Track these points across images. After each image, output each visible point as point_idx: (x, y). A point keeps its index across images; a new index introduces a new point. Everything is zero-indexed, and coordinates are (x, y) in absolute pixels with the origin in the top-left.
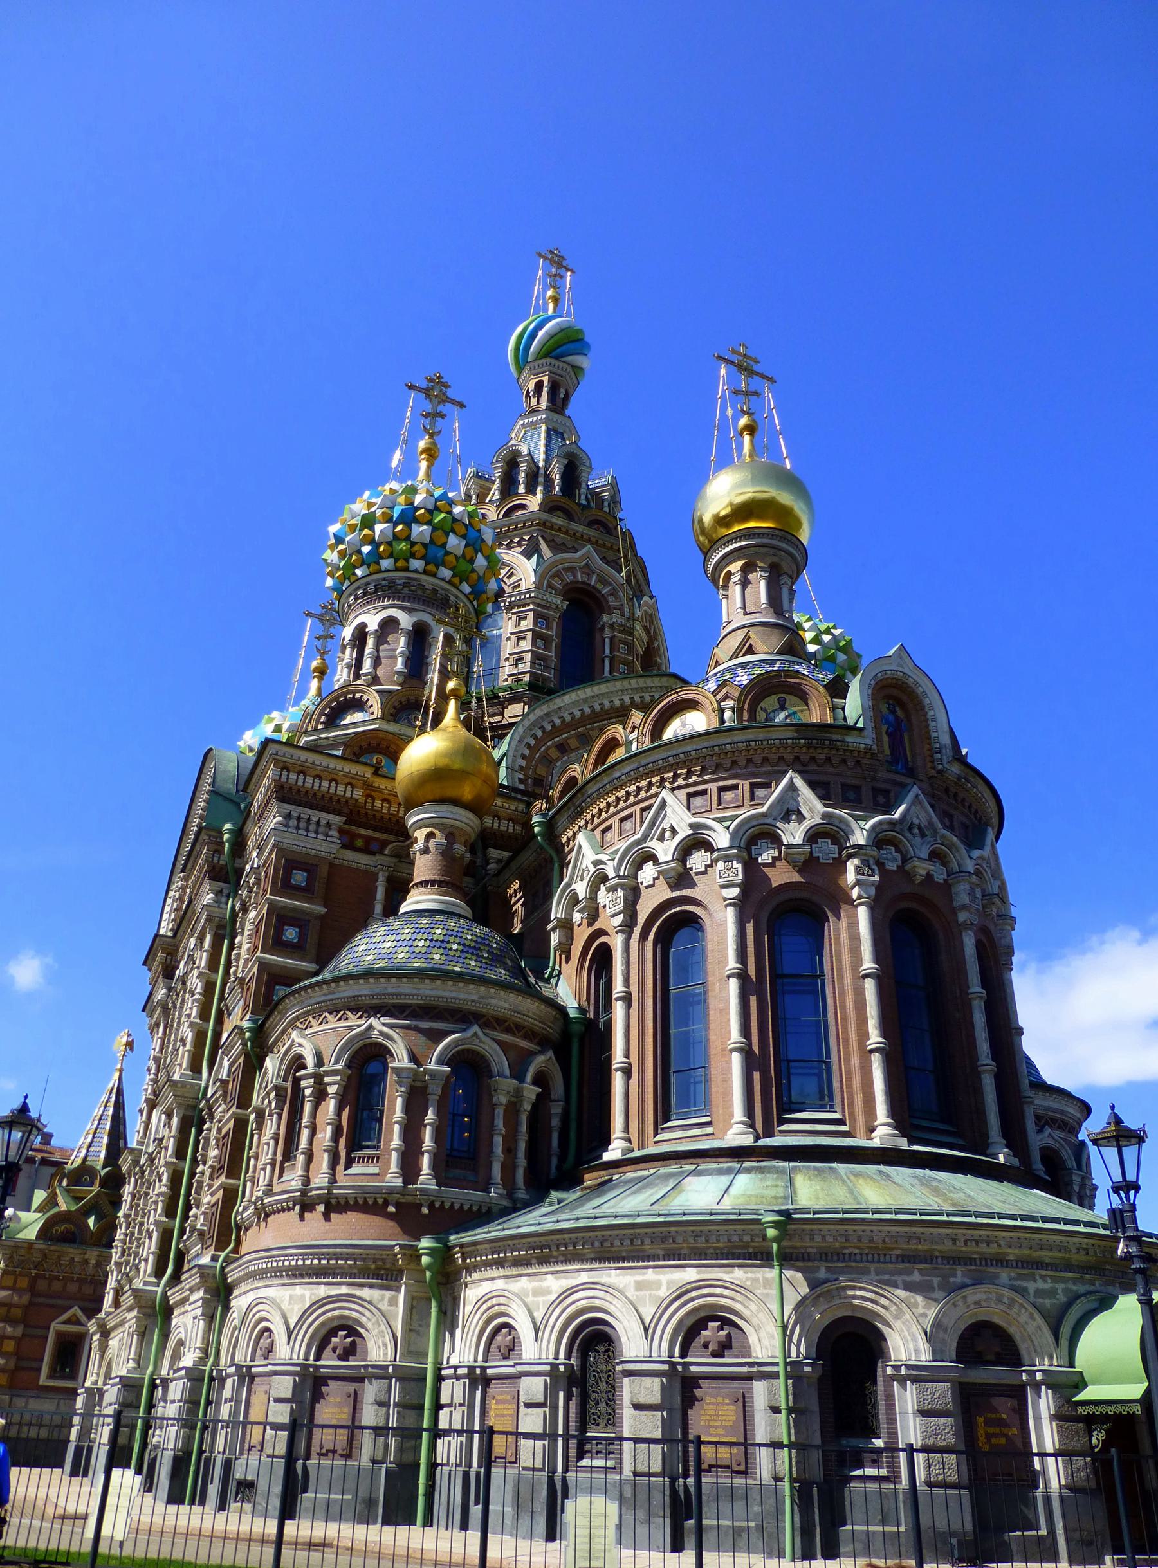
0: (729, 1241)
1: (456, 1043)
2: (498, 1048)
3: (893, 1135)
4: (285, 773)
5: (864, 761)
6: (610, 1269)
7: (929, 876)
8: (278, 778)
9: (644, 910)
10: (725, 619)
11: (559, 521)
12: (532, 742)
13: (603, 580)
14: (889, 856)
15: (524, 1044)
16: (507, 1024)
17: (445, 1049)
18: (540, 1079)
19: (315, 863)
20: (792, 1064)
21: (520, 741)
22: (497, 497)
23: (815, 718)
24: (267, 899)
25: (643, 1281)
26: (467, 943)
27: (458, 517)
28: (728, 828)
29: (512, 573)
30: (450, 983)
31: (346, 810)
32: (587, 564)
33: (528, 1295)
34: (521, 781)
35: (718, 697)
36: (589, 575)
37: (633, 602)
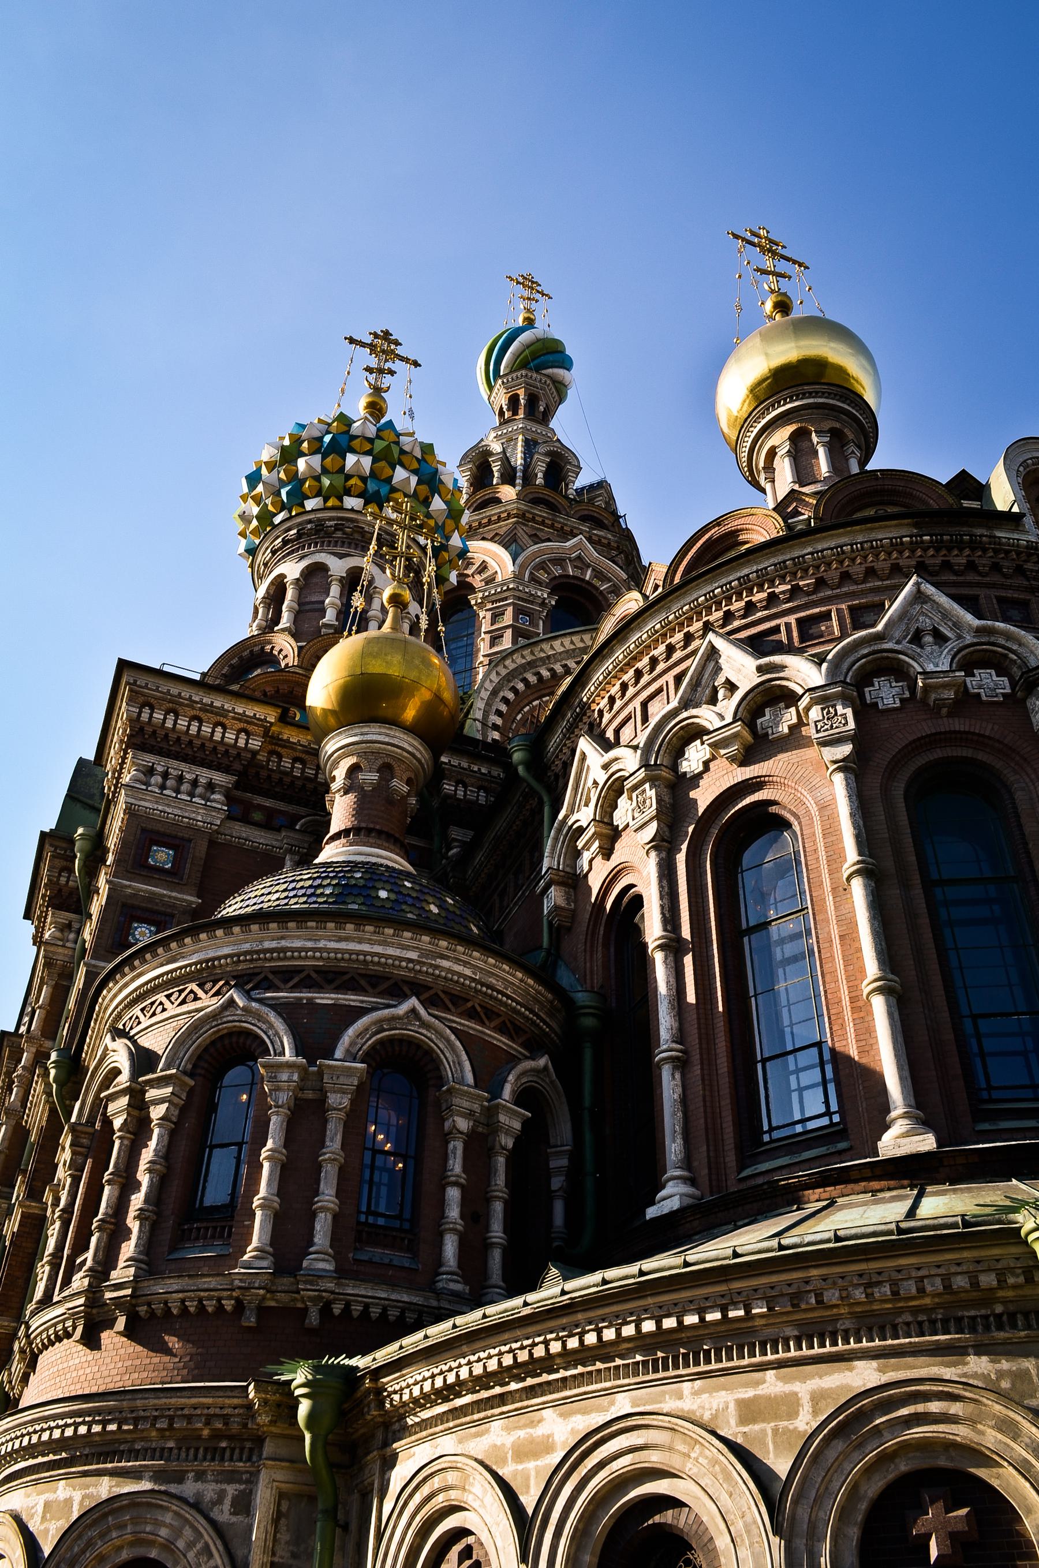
0: (947, 1287)
1: (380, 1025)
2: (453, 1037)
6: (679, 1379)
11: (541, 512)
13: (599, 574)
15: (501, 1041)
16: (469, 1005)
19: (187, 836)
21: (494, 693)
25: (756, 1399)
27: (407, 448)
30: (370, 928)
31: (237, 766)
32: (579, 557)
33: (504, 1461)
36: (581, 569)
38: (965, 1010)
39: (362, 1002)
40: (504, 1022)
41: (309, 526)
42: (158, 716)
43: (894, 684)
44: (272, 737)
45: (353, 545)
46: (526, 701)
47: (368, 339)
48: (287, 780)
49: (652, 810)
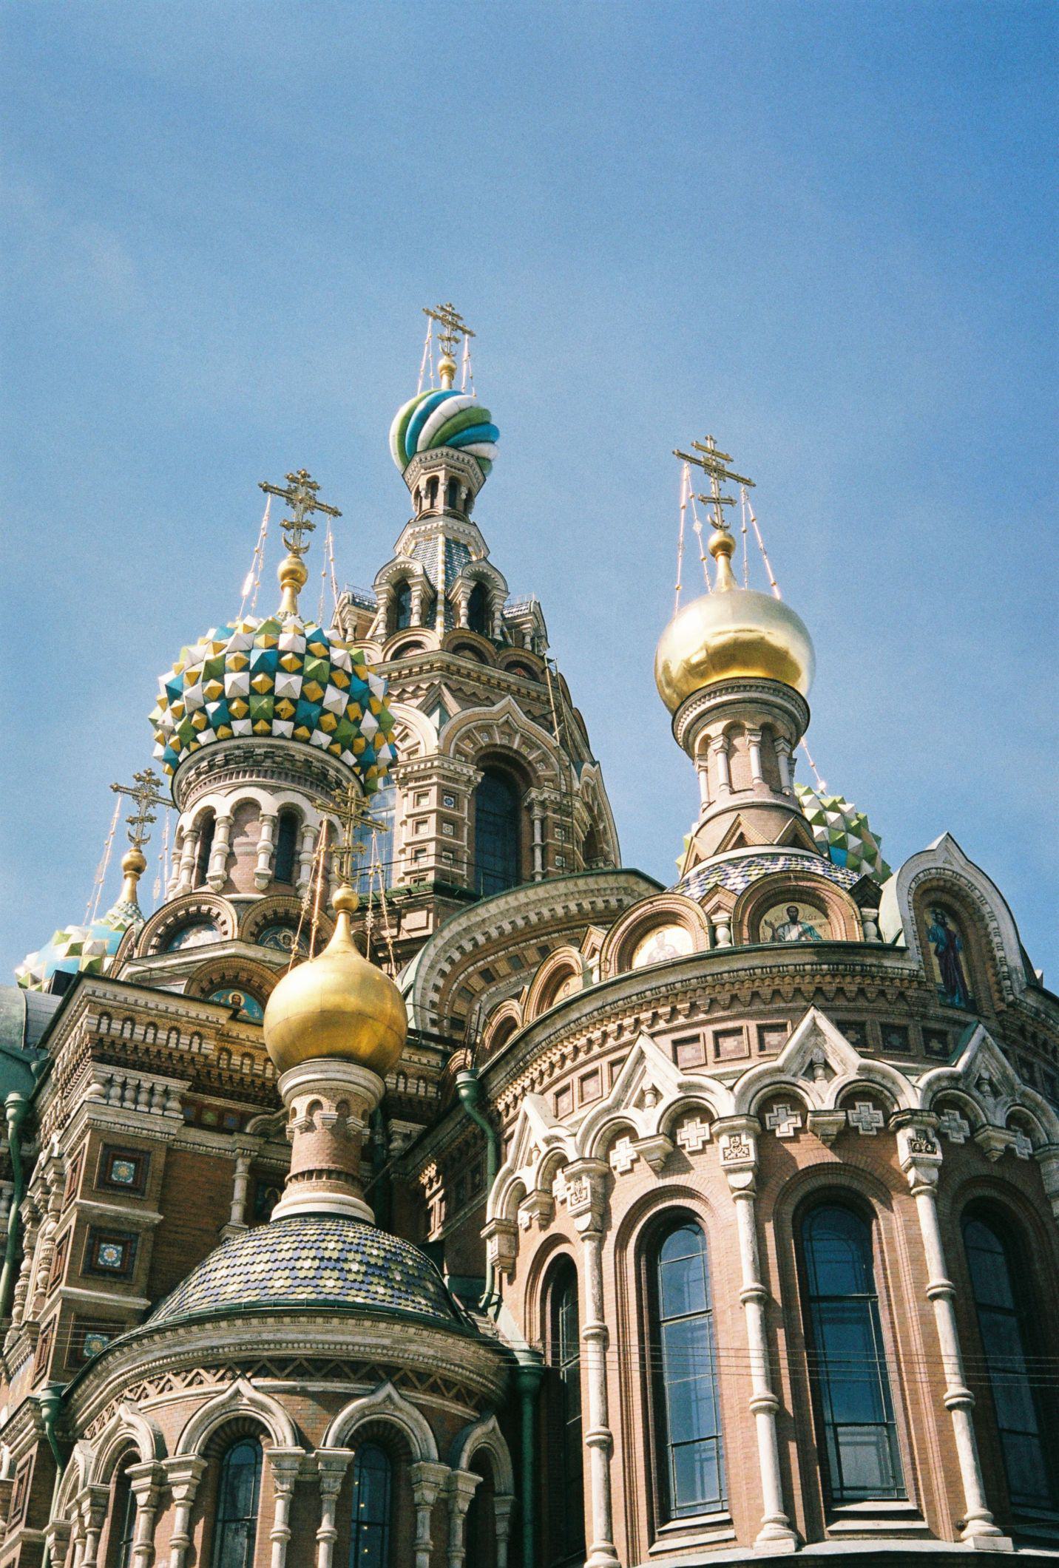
1: (362, 1412)
2: (421, 1418)
3: (992, 1534)
4: (105, 1021)
5: (910, 993)
7: (1009, 1151)
8: (94, 1028)
9: (621, 1205)
10: (704, 798)
12: (447, 968)
13: (527, 741)
14: (953, 1124)
15: (457, 1409)
16: (431, 1380)
17: (345, 1423)
18: (481, 1463)
19: (146, 1149)
20: (840, 1429)
21: (432, 967)
22: (381, 630)
23: (840, 936)
24: (77, 1204)
26: (373, 1261)
27: (338, 664)
28: (731, 1089)
29: (407, 735)
30: (352, 1322)
31: (191, 1071)
32: (507, 722)
34: (434, 1022)
35: (708, 908)
36: (509, 735)
37: (571, 771)
38: (828, 1417)
39: (346, 1388)
40: (459, 1390)
41: (237, 752)
42: (116, 1025)
43: (790, 1112)
44: (222, 1035)
45: (283, 776)
46: (461, 969)
47: (284, 485)
48: (237, 1077)
49: (587, 1203)
